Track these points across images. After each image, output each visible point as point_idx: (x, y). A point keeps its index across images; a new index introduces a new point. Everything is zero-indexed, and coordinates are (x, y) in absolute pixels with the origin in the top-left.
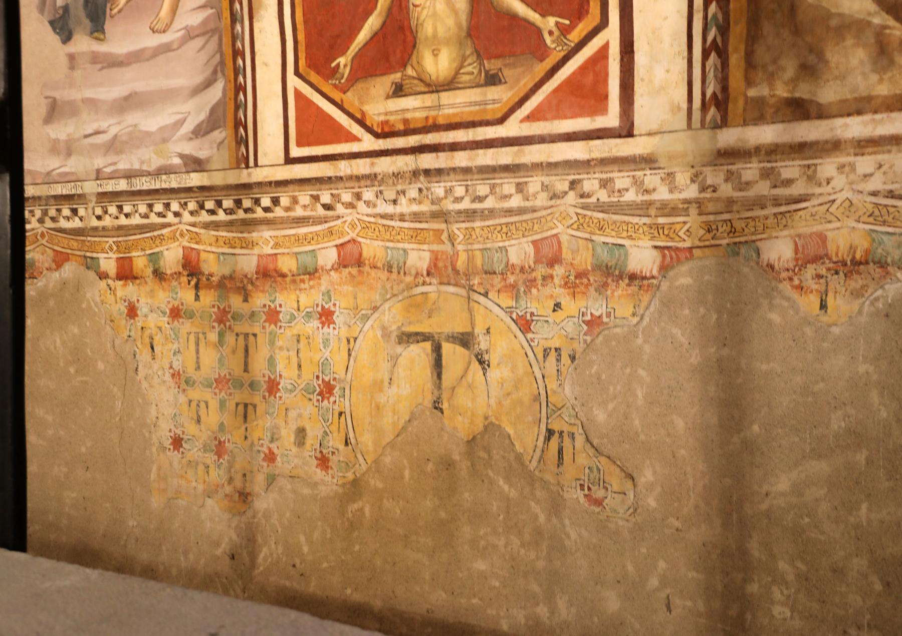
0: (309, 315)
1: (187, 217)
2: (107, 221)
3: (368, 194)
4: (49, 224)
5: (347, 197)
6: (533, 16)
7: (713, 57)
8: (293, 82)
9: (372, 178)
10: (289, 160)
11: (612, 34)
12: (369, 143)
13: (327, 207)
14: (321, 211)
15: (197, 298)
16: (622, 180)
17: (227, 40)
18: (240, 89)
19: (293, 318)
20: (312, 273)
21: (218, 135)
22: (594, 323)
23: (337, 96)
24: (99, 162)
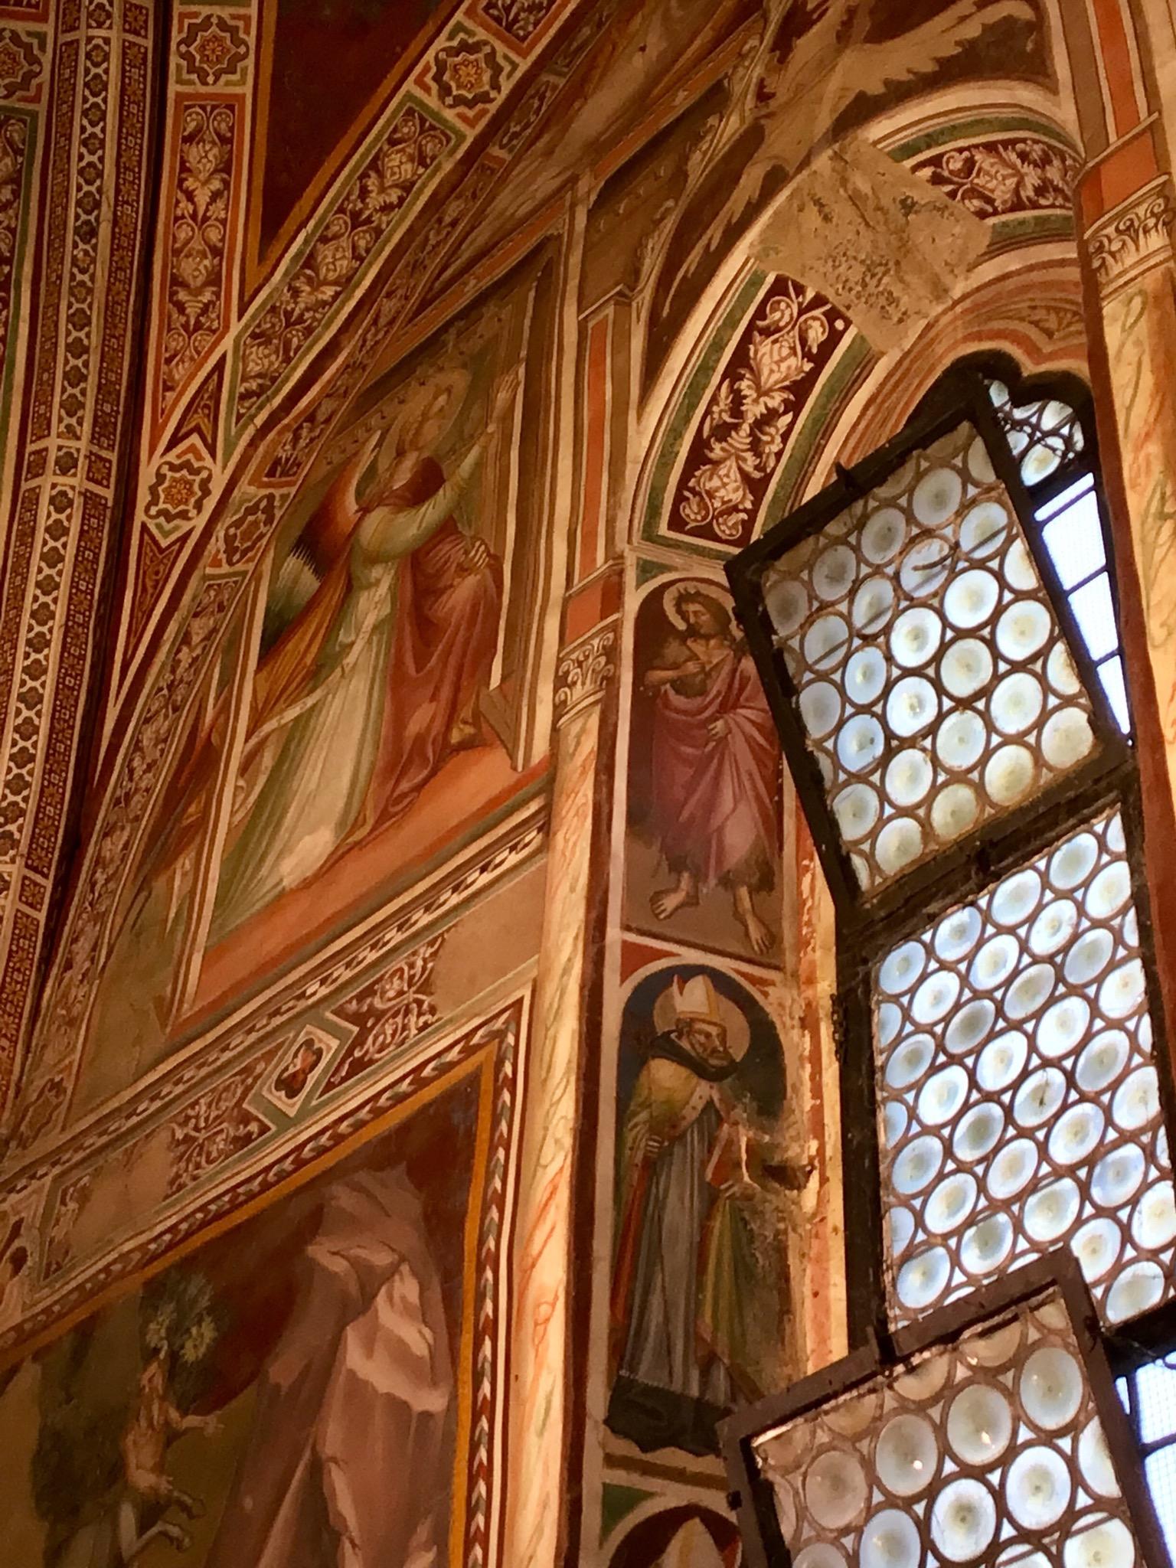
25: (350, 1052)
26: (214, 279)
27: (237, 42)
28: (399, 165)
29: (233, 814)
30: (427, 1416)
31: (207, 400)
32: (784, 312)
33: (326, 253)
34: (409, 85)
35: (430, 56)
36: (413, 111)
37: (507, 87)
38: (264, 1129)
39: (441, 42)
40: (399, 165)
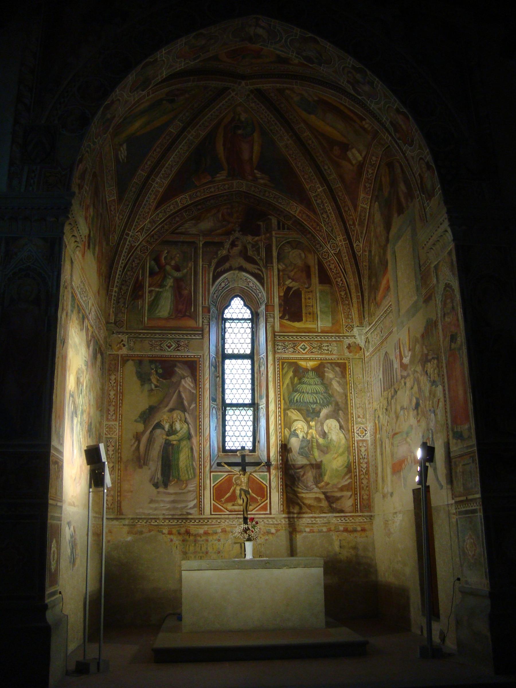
0: (216, 540)
1: (187, 523)
2: (165, 523)
3: (227, 521)
4: (148, 523)
5: (223, 521)
6: (257, 497)
7: (282, 506)
8: (212, 502)
9: (228, 518)
10: (211, 514)
11: (268, 501)
12: (228, 513)
13: (219, 522)
14: (218, 523)
15: (189, 538)
16: (270, 520)
17: (198, 493)
18: (200, 502)
19: (212, 541)
20: (216, 533)
21: (196, 509)
22: (266, 540)
23: (222, 505)
24: (164, 512)
25: (177, 348)
26: (148, 213)
27: (163, 185)
28: (172, 207)
29: (148, 299)
30: (193, 393)
31: (143, 229)
32: (226, 281)
33: (160, 214)
34: (178, 199)
35: (181, 197)
36: (176, 202)
37: (187, 204)
38: (165, 350)
39: (183, 196)
40: (172, 207)
